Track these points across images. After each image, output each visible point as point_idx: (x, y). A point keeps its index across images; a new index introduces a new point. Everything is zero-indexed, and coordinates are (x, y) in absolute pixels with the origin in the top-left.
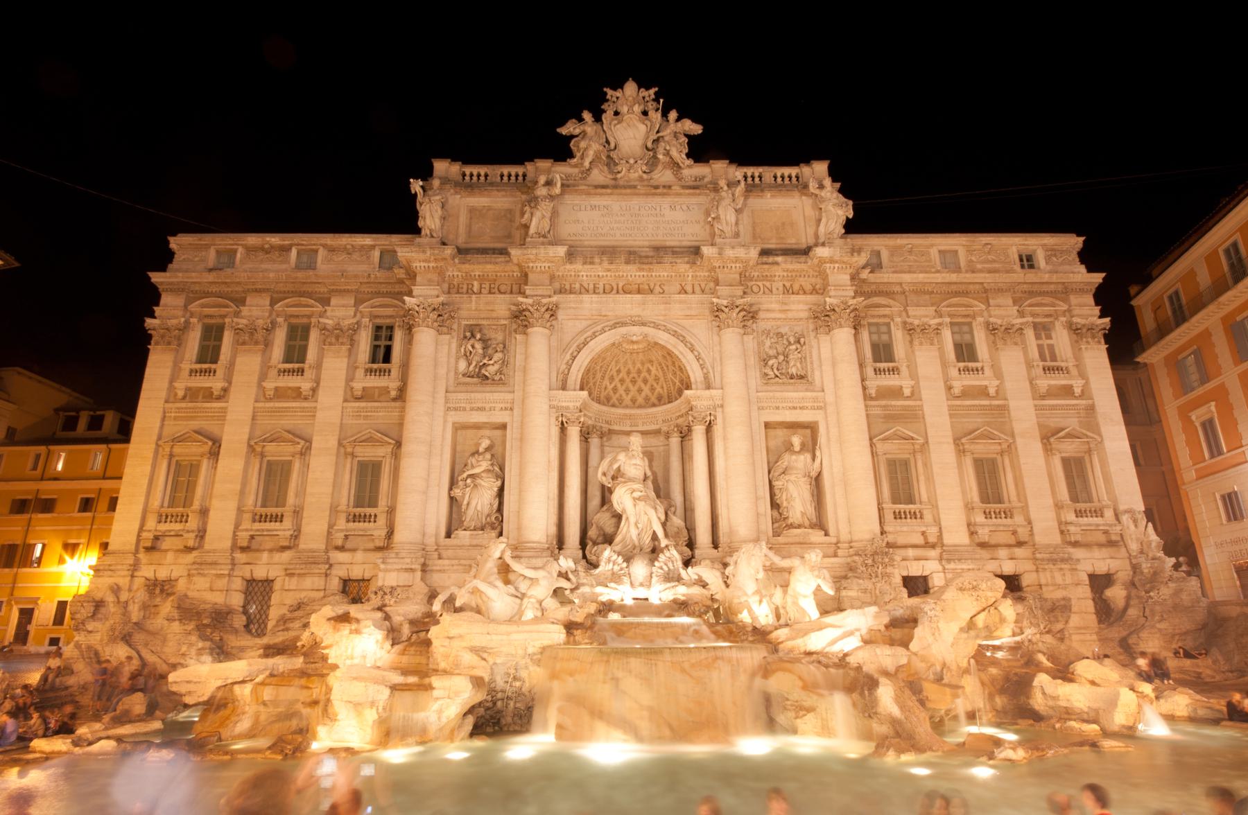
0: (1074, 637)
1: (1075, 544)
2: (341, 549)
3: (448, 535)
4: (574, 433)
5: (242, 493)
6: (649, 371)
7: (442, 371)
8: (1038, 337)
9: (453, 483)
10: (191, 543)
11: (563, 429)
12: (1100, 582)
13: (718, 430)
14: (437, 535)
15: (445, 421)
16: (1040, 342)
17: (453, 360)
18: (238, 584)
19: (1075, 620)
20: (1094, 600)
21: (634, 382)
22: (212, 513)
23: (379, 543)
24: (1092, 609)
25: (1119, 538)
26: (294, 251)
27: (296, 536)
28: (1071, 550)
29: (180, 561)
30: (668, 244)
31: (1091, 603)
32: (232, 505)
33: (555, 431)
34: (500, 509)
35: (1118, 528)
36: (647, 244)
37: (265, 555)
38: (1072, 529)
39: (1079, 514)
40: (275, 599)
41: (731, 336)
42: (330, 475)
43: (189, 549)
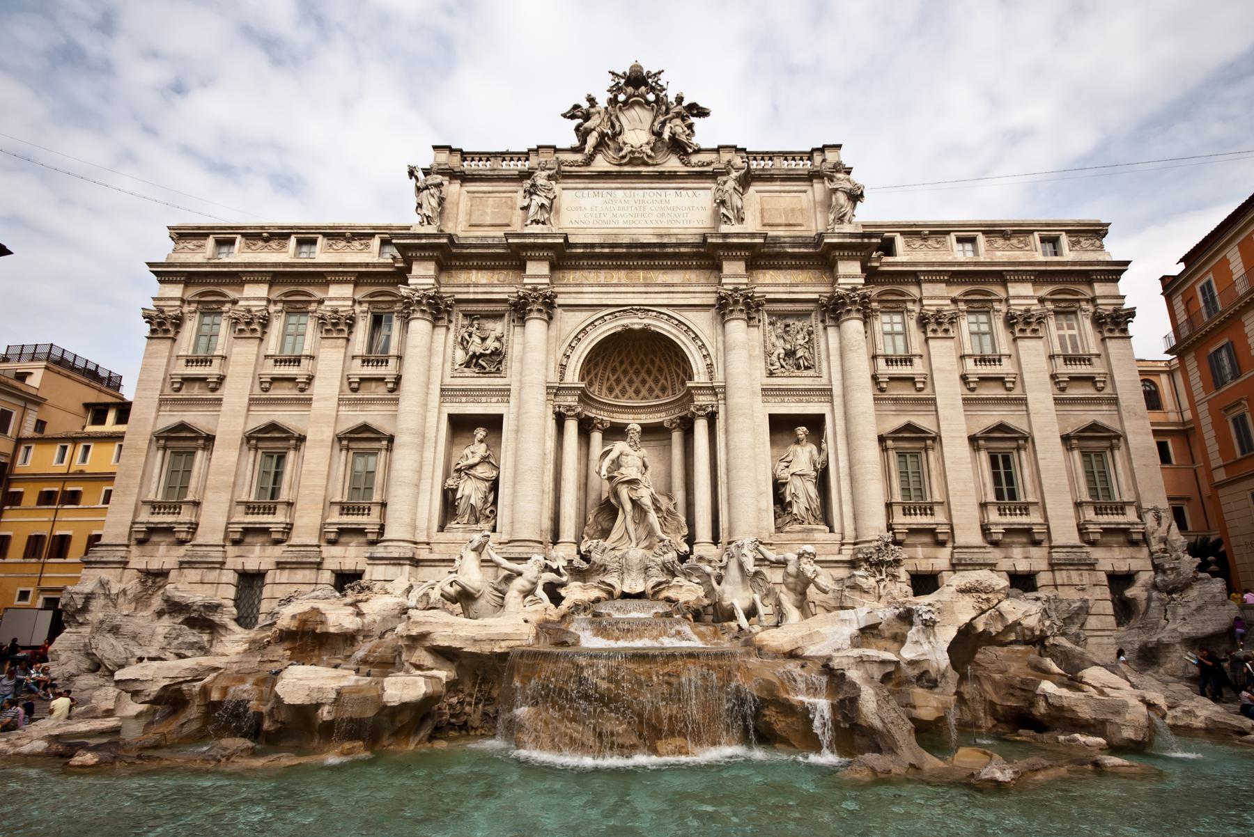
0: (1090, 640)
1: (1093, 544)
2: (333, 543)
4: (571, 427)
9: (447, 475)
10: (183, 536)
12: (1118, 581)
13: (720, 424)
15: (439, 413)
19: (1092, 622)
20: (1112, 601)
22: (204, 505)
23: (371, 537)
24: (1111, 611)
25: (1140, 537)
28: (1089, 549)
29: (172, 553)
30: (672, 231)
31: (1110, 604)
32: (225, 497)
33: (551, 424)
34: (495, 502)
36: (651, 231)
37: (257, 549)
38: (1091, 528)
40: (267, 592)
41: (737, 327)
43: (182, 543)
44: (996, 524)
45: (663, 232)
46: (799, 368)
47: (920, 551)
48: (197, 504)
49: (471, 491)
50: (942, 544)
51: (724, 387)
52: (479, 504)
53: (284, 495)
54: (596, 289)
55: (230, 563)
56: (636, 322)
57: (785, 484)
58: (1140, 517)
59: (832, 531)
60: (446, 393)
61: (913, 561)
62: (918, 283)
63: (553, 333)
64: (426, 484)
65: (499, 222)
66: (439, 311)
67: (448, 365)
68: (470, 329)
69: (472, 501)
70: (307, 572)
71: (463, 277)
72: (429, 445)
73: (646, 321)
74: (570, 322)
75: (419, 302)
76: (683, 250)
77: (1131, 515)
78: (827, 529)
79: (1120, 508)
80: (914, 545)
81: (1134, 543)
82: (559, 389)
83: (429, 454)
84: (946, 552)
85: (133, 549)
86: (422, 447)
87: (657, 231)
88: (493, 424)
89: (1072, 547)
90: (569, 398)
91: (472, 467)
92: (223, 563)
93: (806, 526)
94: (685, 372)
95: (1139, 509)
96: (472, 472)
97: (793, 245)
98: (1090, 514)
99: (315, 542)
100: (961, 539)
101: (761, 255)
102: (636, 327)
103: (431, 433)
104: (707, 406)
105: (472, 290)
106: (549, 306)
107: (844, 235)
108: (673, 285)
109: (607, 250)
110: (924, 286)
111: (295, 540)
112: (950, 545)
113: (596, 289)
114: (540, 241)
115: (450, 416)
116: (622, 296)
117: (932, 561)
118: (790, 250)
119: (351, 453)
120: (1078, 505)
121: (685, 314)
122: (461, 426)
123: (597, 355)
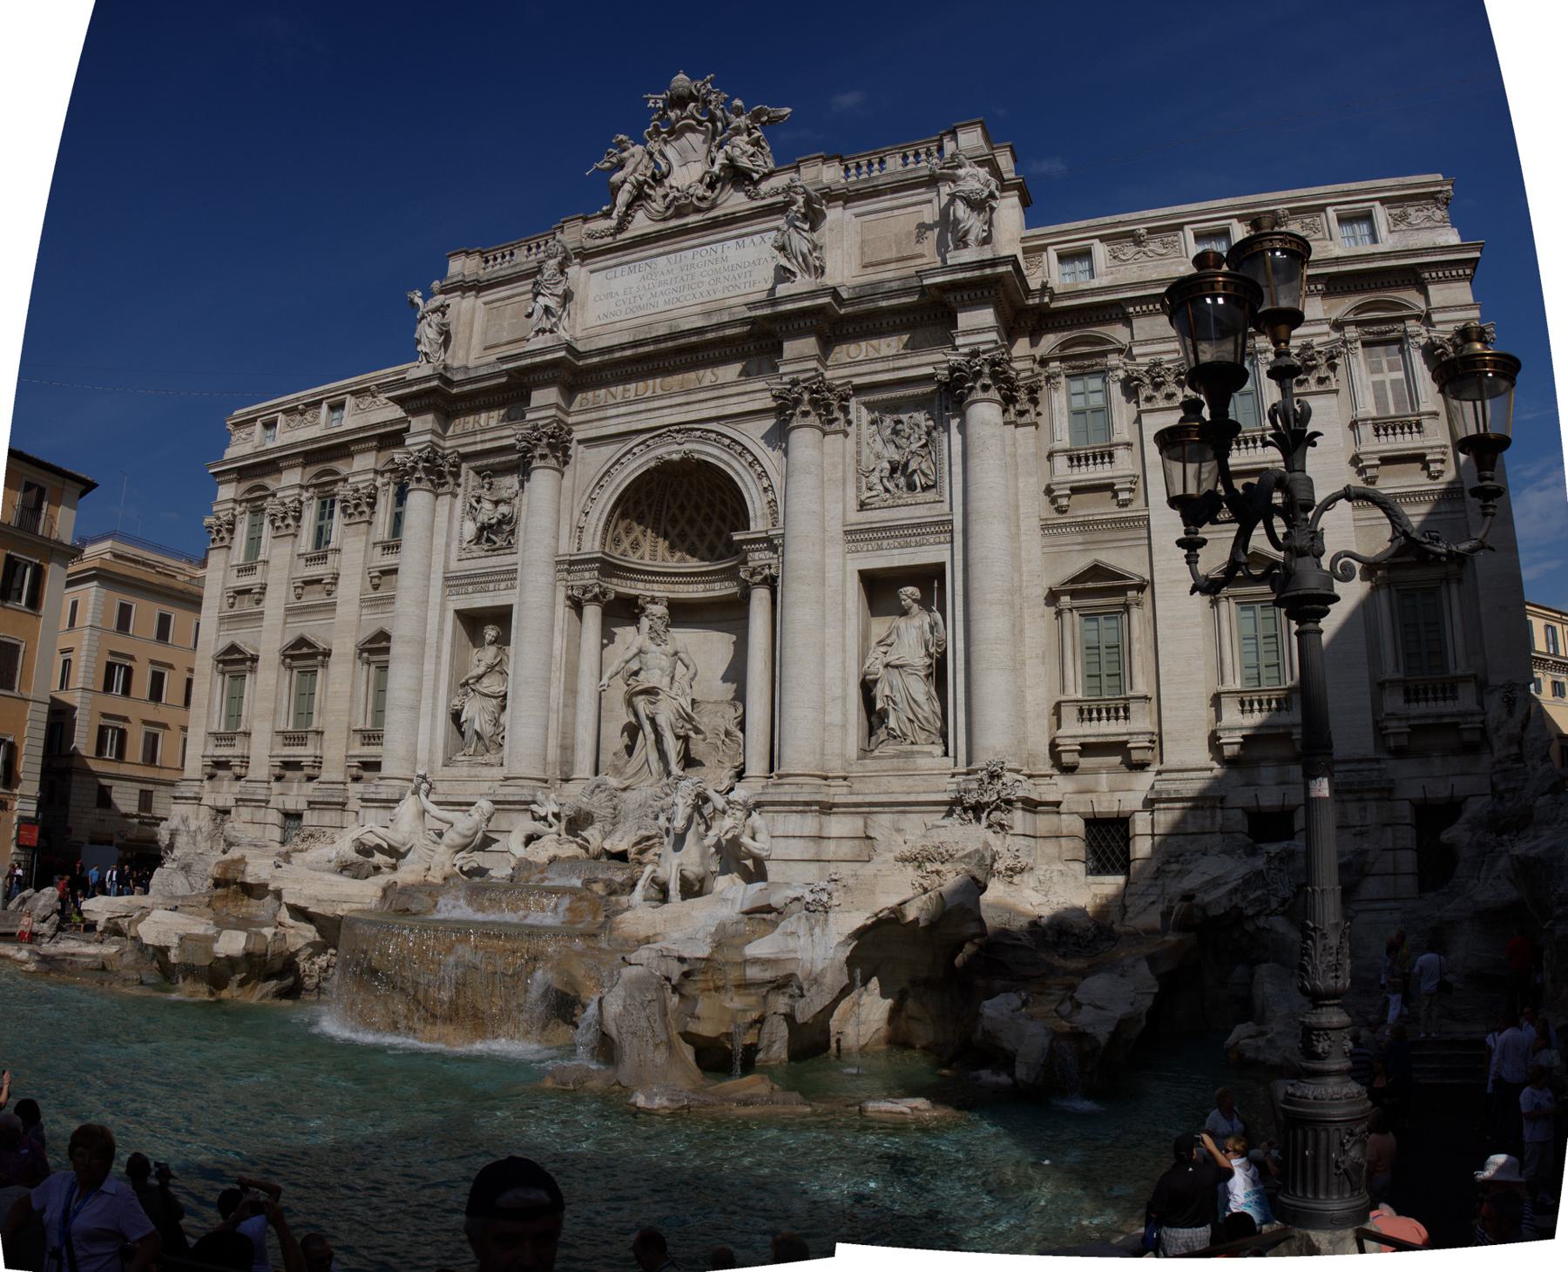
1: (1400, 753)
2: (356, 779)
3: (448, 762)
5: (275, 712)
6: (723, 502)
7: (440, 541)
8: (1377, 369)
11: (577, 606)
14: (431, 761)
16: (1378, 377)
17: (456, 524)
18: (274, 817)
21: (708, 520)
26: (325, 406)
27: (318, 763)
33: (562, 611)
35: (1478, 719)
36: (698, 309)
38: (1393, 726)
39: (1411, 695)
42: (346, 688)
44: (1230, 729)
45: (715, 306)
46: (911, 487)
47: (1104, 780)
48: (247, 734)
49: (477, 713)
50: (1141, 766)
51: (783, 536)
52: (488, 730)
53: (316, 724)
54: (622, 410)
55: (276, 801)
56: (671, 451)
57: (875, 682)
58: (1481, 703)
59: (946, 754)
60: (453, 582)
61: (1089, 796)
62: (1127, 321)
63: (567, 482)
64: (426, 707)
65: (517, 336)
66: (441, 475)
67: (455, 546)
68: (479, 492)
69: (477, 727)
70: (333, 814)
71: (470, 422)
72: (430, 652)
73: (687, 447)
74: (586, 462)
75: (414, 469)
76: (728, 332)
77: (1466, 699)
78: (939, 750)
79: (1448, 689)
80: (1095, 771)
81: (1471, 749)
82: (571, 563)
83: (429, 666)
84: (1143, 782)
85: (206, 783)
86: (420, 659)
87: (708, 307)
88: (502, 617)
89: (1360, 761)
90: (587, 575)
91: (479, 678)
92: (268, 802)
93: (906, 747)
94: (735, 514)
95: (1482, 686)
96: (477, 687)
97: (889, 294)
98: (1394, 702)
99: (341, 779)
100: (1172, 758)
101: (836, 322)
102: (675, 457)
103: (432, 637)
104: (762, 567)
105: (479, 438)
106: (559, 446)
107: (964, 267)
108: (723, 386)
109: (628, 353)
110: (1136, 323)
111: (324, 776)
112: (1156, 767)
113: (622, 410)
114: (538, 359)
115: (457, 612)
116: (657, 413)
117: (1118, 795)
118: (884, 304)
119: (373, 667)
120: (1380, 686)
121: (743, 427)
122: (473, 622)
123: (637, 503)
